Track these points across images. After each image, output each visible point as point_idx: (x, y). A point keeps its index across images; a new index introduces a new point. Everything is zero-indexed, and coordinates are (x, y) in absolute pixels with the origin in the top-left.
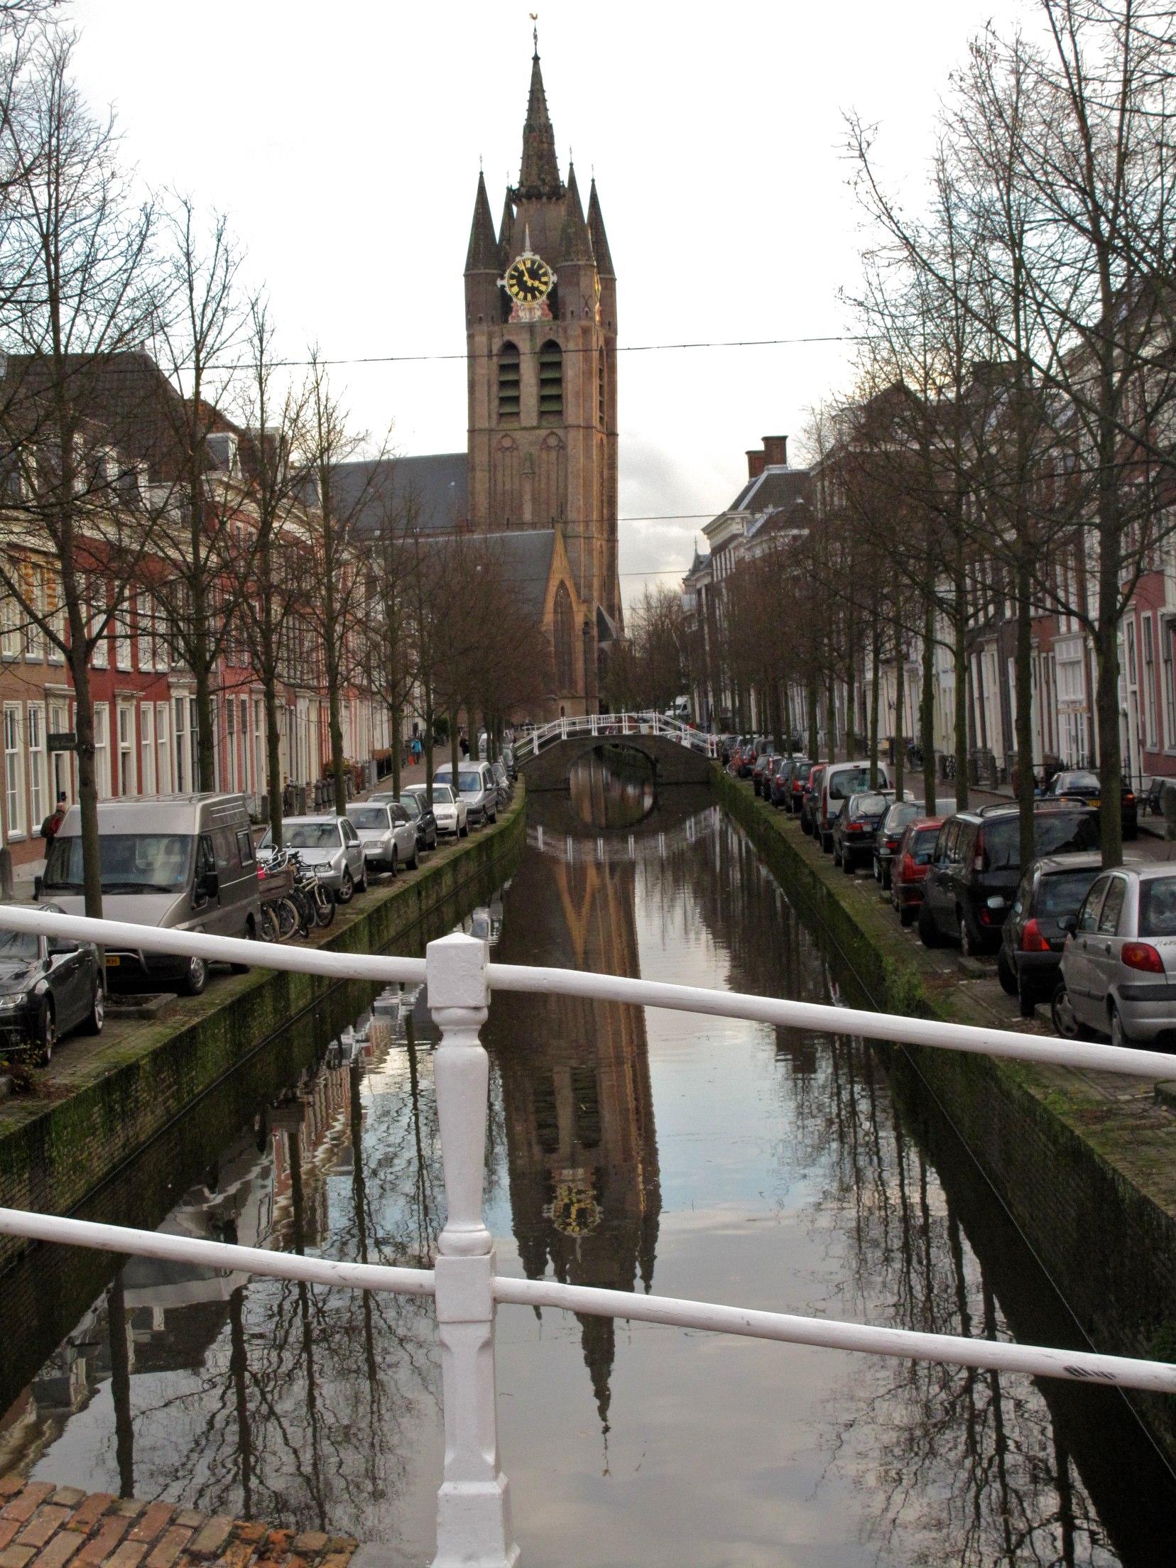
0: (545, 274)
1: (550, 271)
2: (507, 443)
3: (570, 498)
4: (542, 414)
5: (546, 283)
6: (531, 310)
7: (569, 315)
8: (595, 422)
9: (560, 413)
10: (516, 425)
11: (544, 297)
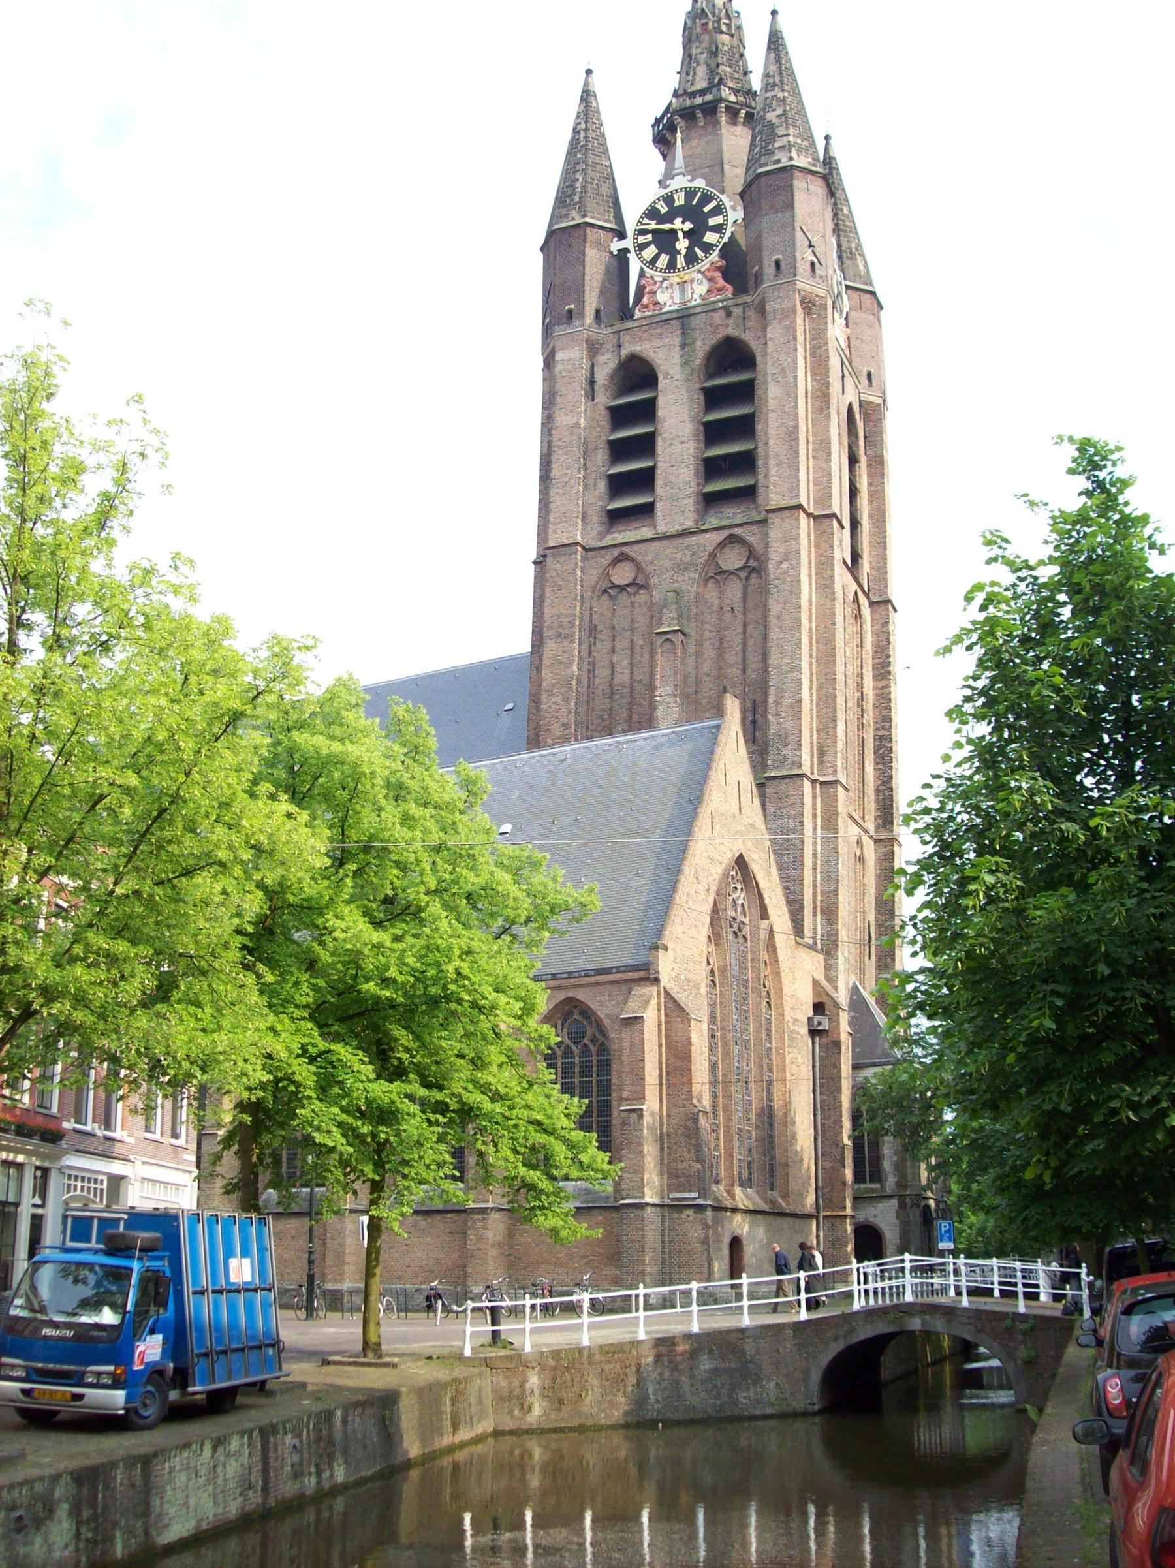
0: (718, 210)
2: (623, 575)
3: (773, 681)
4: (710, 500)
5: (719, 229)
7: (769, 270)
8: (839, 504)
9: (748, 494)
10: (646, 532)
11: (715, 256)
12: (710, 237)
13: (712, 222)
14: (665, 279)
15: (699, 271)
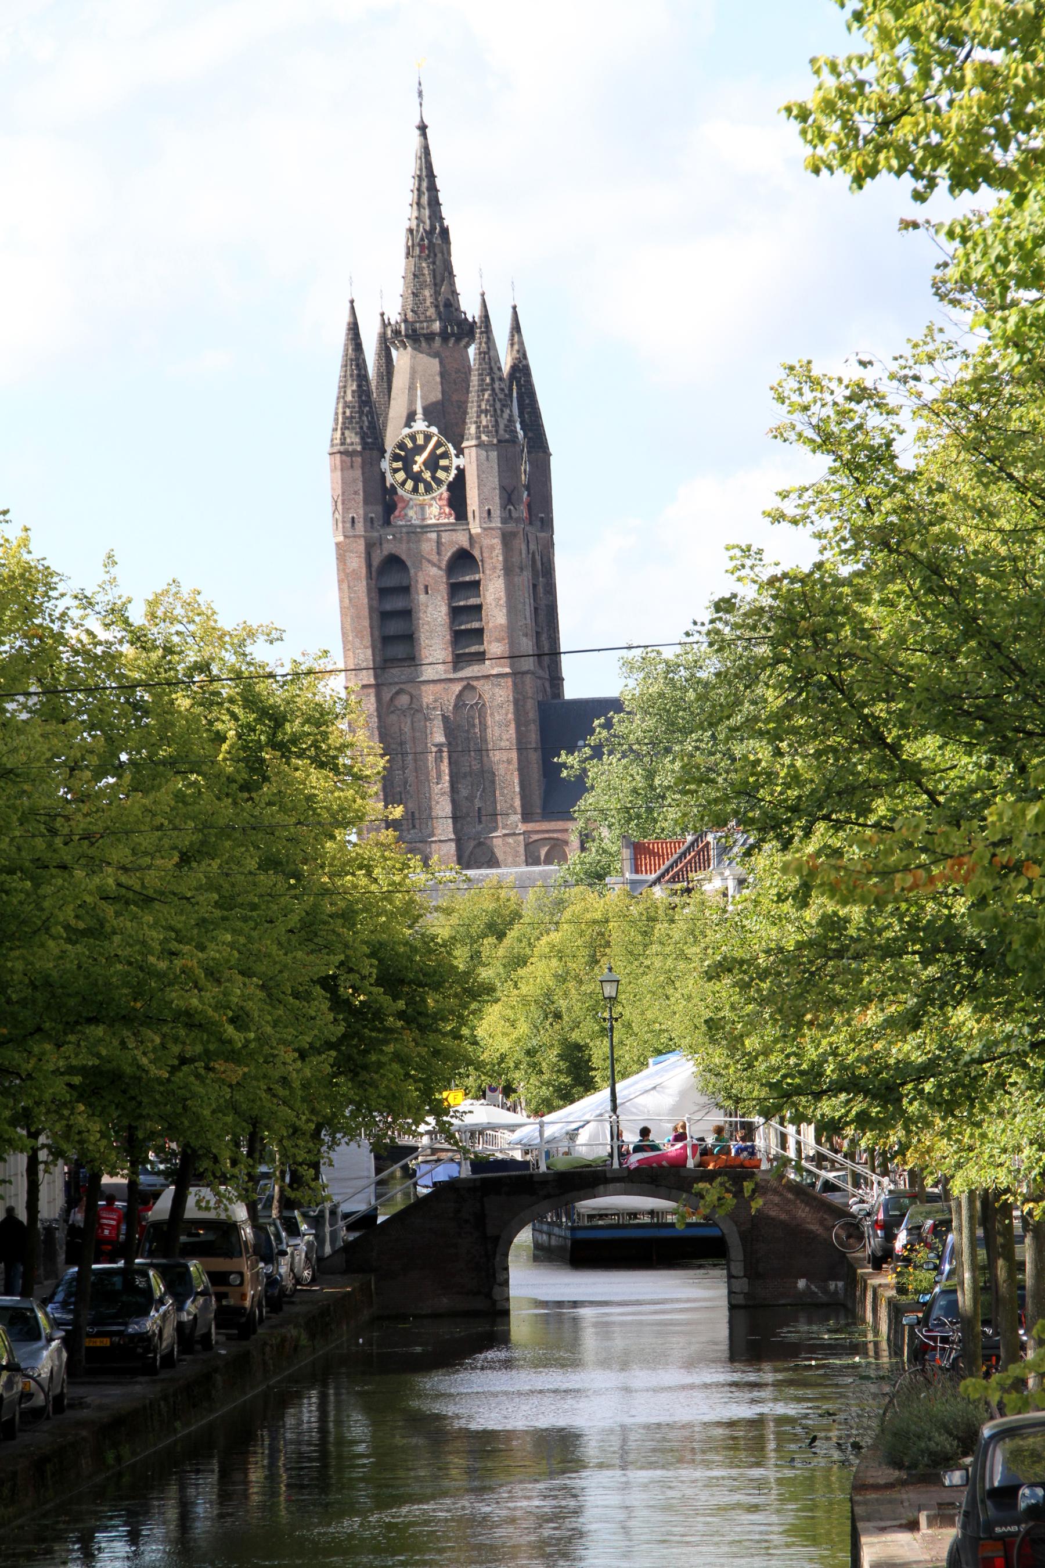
0: (445, 455)
1: (453, 451)
5: (446, 469)
6: (422, 507)
11: (444, 488)
12: (441, 474)
13: (443, 462)
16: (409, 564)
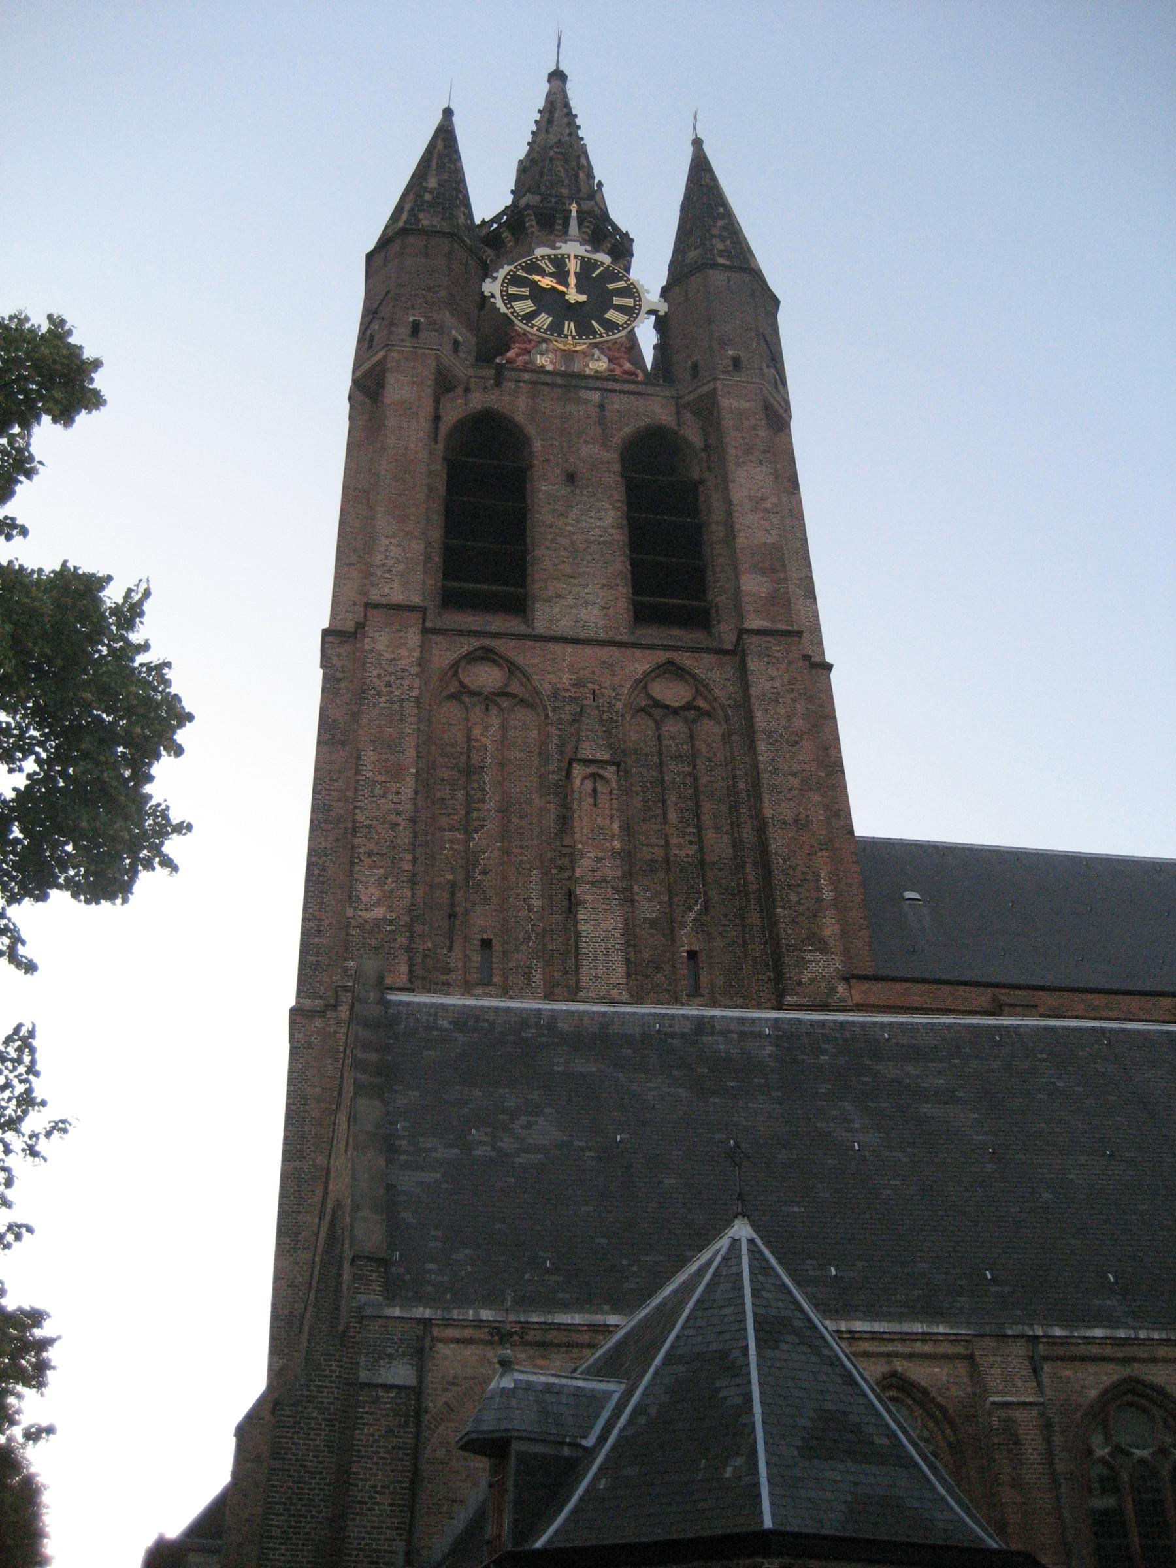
13: (617, 301)
14: (544, 340)
15: (596, 345)
16: (531, 430)
